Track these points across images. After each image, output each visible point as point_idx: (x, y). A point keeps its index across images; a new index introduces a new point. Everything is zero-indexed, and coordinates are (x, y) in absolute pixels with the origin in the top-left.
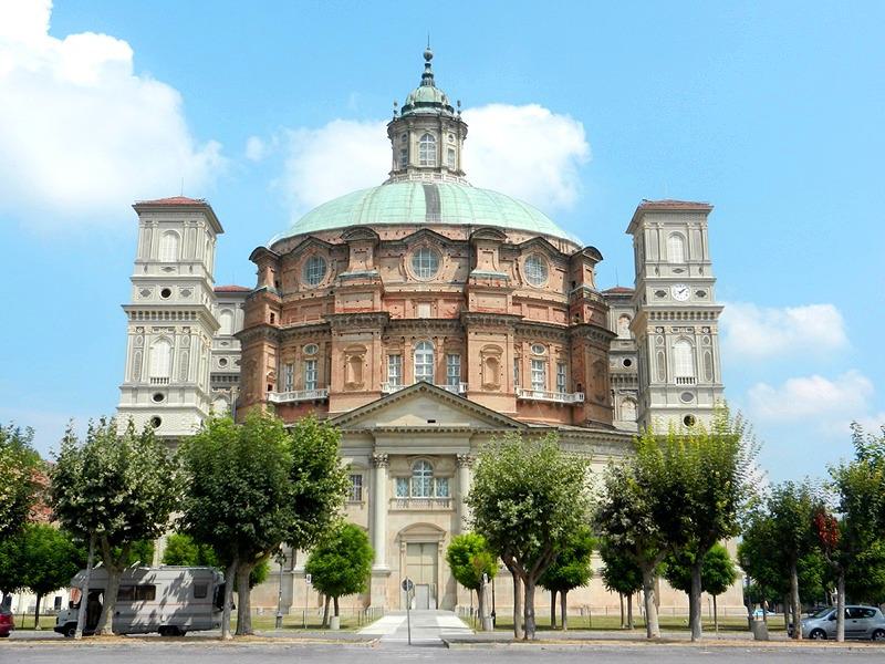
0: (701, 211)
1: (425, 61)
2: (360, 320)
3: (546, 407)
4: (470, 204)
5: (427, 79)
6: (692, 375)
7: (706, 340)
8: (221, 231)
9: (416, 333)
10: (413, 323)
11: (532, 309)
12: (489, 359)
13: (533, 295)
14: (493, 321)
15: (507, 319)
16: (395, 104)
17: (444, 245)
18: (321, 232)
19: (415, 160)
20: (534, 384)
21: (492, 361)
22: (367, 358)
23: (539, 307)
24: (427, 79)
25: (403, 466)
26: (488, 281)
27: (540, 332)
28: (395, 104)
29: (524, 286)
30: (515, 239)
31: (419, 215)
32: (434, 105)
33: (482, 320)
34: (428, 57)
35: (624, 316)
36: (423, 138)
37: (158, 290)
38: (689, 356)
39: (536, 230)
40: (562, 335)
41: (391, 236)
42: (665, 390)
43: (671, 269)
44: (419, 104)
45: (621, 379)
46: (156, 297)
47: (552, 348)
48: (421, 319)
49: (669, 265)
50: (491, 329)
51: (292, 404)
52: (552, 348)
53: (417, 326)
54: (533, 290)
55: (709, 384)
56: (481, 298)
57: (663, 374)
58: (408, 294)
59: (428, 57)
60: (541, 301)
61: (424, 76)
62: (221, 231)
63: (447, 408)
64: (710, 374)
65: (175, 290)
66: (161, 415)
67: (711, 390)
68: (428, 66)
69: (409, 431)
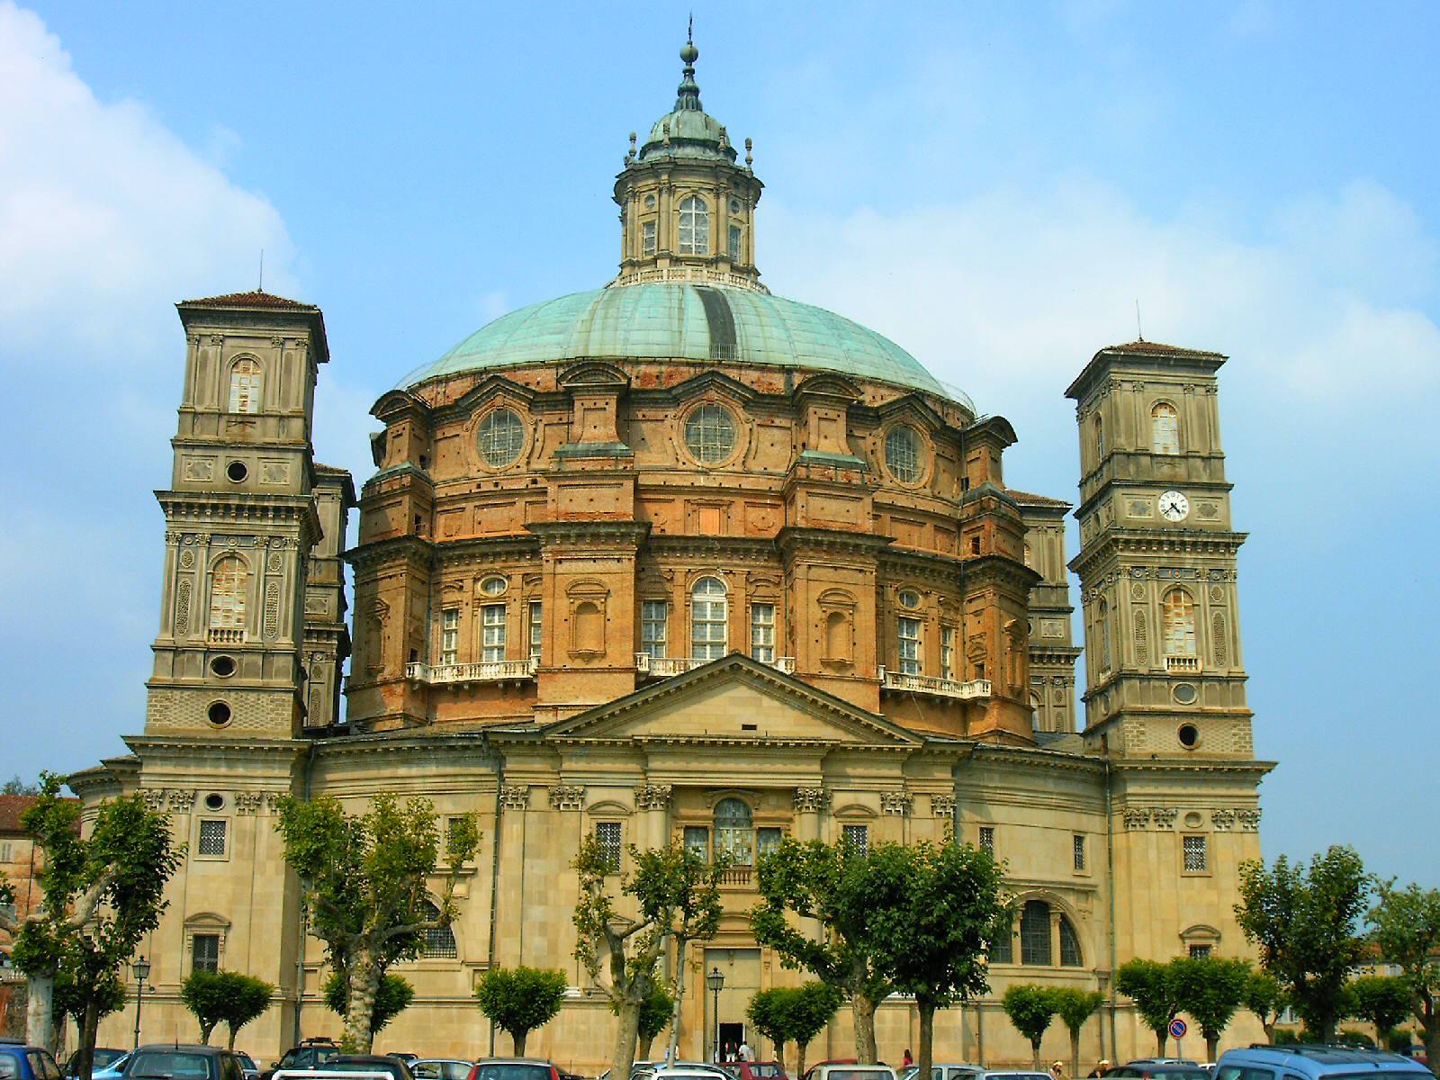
0: (1210, 363)
1: (683, 65)
3: (919, 707)
4: (787, 330)
5: (689, 96)
9: (696, 562)
10: (690, 544)
13: (902, 501)
16: (633, 139)
18: (515, 368)
24: (689, 96)
25: (700, 812)
26: (831, 472)
27: (914, 568)
28: (633, 139)
30: (870, 398)
31: (697, 341)
32: (704, 144)
34: (690, 57)
36: (686, 203)
40: (949, 574)
44: (679, 142)
48: (706, 538)
51: (458, 687)
52: (933, 599)
53: (697, 549)
58: (679, 490)
60: (914, 511)
63: (776, 703)
66: (230, 700)
68: (689, 73)
69: (714, 743)
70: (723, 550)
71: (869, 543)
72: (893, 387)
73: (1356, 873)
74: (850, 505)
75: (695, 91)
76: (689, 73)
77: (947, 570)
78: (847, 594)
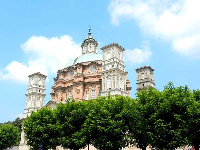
1: (89, 31)
2: (57, 89)
6: (110, 88)
8: (153, 70)
9: (69, 89)
12: (77, 92)
14: (77, 84)
15: (80, 82)
17: (74, 69)
20: (93, 96)
21: (78, 93)
22: (58, 96)
29: (90, 74)
33: (75, 84)
34: (90, 30)
35: (143, 73)
36: (85, 47)
37: (38, 90)
38: (110, 83)
39: (91, 60)
41: (66, 70)
42: (104, 93)
43: (107, 62)
45: (144, 89)
46: (30, 92)
47: (97, 87)
49: (107, 61)
50: (78, 86)
52: (97, 87)
54: (93, 74)
55: (114, 89)
56: (76, 79)
57: (104, 89)
59: (90, 30)
62: (153, 70)
65: (32, 90)
67: (114, 90)
68: (90, 31)
70: (71, 87)
74: (80, 78)
76: (90, 31)
78: (79, 89)
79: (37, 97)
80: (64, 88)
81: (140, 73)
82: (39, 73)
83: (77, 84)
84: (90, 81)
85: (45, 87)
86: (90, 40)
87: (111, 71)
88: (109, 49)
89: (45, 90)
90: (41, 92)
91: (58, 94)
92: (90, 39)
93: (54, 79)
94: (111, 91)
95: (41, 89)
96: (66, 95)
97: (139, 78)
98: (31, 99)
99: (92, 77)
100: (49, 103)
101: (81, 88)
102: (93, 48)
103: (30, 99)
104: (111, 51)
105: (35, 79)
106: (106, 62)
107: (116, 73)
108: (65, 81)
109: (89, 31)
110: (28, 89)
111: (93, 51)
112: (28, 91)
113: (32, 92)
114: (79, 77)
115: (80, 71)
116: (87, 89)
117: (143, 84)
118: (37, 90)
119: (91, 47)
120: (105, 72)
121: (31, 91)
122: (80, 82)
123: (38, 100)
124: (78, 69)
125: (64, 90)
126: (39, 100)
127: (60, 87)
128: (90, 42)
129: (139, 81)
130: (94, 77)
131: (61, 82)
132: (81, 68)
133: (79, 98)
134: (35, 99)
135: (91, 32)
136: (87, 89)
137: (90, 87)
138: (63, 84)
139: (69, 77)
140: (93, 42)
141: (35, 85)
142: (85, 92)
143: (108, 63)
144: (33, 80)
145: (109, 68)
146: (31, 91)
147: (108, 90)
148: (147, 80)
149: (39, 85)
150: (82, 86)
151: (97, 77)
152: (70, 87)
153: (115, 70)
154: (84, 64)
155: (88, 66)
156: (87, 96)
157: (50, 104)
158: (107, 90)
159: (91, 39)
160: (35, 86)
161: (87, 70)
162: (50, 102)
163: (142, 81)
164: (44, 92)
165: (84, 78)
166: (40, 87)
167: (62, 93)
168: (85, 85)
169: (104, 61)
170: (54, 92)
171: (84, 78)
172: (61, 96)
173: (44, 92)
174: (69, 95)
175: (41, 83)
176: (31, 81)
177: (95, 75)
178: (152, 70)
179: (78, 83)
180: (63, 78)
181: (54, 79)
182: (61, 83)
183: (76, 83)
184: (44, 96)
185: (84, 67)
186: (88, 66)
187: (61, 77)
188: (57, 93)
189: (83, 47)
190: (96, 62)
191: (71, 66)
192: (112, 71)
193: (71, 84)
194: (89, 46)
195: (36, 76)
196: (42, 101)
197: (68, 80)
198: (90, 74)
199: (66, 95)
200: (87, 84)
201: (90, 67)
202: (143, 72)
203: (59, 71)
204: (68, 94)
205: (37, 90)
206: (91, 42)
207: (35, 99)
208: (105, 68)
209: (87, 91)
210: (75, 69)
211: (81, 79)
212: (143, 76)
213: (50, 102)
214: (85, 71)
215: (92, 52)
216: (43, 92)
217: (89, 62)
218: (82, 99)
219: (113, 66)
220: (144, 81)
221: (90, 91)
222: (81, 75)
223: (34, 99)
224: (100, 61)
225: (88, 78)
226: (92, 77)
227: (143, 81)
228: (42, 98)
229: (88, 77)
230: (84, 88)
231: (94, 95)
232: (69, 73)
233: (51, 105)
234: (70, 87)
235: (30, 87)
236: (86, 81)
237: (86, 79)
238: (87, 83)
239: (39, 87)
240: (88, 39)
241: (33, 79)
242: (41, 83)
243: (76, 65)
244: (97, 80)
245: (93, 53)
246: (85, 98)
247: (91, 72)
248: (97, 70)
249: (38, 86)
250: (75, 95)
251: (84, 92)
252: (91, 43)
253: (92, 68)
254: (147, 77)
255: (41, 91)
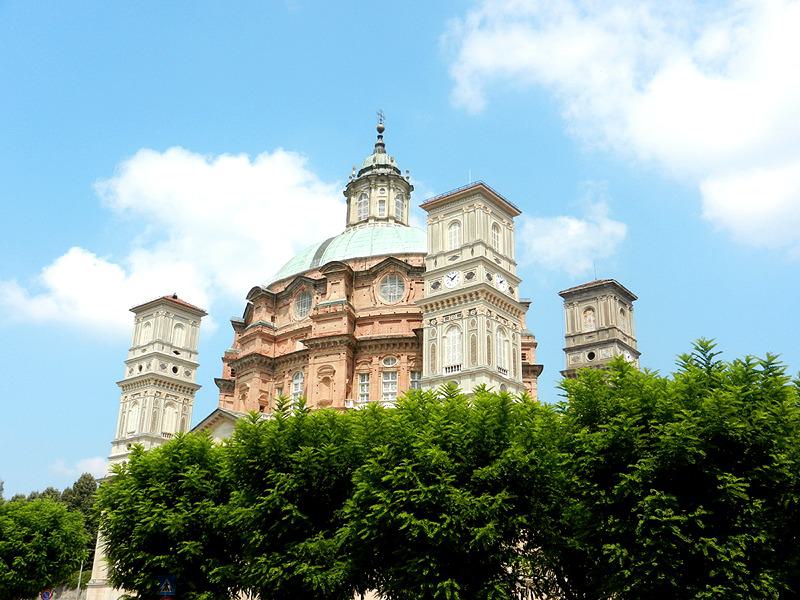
7: (473, 323)
8: (633, 298)
11: (385, 325)
13: (386, 312)
15: (336, 340)
19: (352, 221)
20: (387, 394)
21: (326, 380)
22: (248, 394)
23: (394, 321)
29: (379, 305)
33: (317, 345)
34: (381, 130)
35: (589, 309)
36: (360, 199)
37: (170, 366)
40: (412, 344)
42: (431, 382)
43: (447, 258)
46: (136, 373)
47: (404, 358)
49: (445, 255)
50: (327, 352)
52: (404, 358)
54: (387, 307)
55: (473, 369)
56: (323, 325)
57: (433, 366)
59: (381, 130)
60: (396, 315)
61: (377, 145)
62: (633, 298)
64: (474, 359)
65: (144, 365)
67: (472, 375)
68: (380, 137)
70: (299, 358)
71: (340, 339)
72: (380, 257)
73: (430, 491)
74: (336, 323)
75: (383, 145)
76: (380, 137)
77: (410, 342)
79: (164, 393)
80: (271, 359)
81: (578, 309)
82: (175, 297)
83: (323, 343)
84: (375, 335)
85: (197, 354)
86: (382, 170)
87: (461, 294)
88: (454, 207)
89: (195, 366)
90: (180, 375)
91: (248, 385)
92: (379, 166)
93: (236, 325)
94: (459, 377)
95: (182, 362)
96: (281, 389)
97: (573, 328)
98: (140, 401)
99: (383, 319)
100: (211, 419)
101: (338, 363)
102: (393, 203)
103: (136, 403)
104: (466, 215)
105: (156, 323)
106: (444, 262)
107: (481, 307)
108: (276, 334)
109: (379, 137)
110: (130, 362)
111: (390, 213)
112: (128, 369)
113: (144, 372)
114: (335, 316)
115: (336, 292)
116: (365, 367)
117: (590, 350)
118: (163, 367)
119: (382, 198)
120: (438, 300)
121: (141, 368)
122: (336, 340)
123: (166, 405)
124: (329, 285)
125: (271, 367)
126: (170, 404)
127: (255, 354)
128: (383, 178)
129: (576, 338)
130: (396, 318)
131: (262, 335)
132: (342, 283)
133: (330, 403)
134: (157, 402)
135: (384, 141)
136: (363, 368)
137: (375, 359)
138: (270, 343)
139: (294, 316)
140: (392, 178)
141: (156, 345)
142: (357, 380)
143: (452, 263)
144: (148, 324)
145: (453, 283)
146: (141, 368)
147: (448, 374)
148: (606, 337)
149: (171, 346)
150: (344, 356)
151: (404, 320)
152: (295, 359)
153: (477, 294)
154: (357, 268)
155: (372, 274)
156: (362, 396)
157: (214, 422)
158: (445, 374)
159: (385, 166)
160: (156, 348)
161: (365, 290)
162: (216, 415)
163: (584, 341)
164: (193, 372)
165: (355, 322)
166: (176, 353)
167: (265, 382)
168: (356, 349)
169: (436, 257)
170: (233, 374)
171: (355, 322)
172: (261, 391)
173: (193, 372)
174: (293, 389)
175: (180, 337)
176: (144, 331)
177: (399, 311)
178: (626, 297)
179: (329, 343)
180: (268, 319)
181: (236, 325)
182: (259, 340)
183: (319, 342)
184: (191, 389)
185: (353, 276)
186: (372, 274)
187: (262, 316)
188: (246, 378)
189: (354, 200)
190: (403, 259)
191: (304, 273)
192: (465, 297)
193: (299, 346)
194: (376, 194)
195: (162, 311)
196: (185, 409)
197: (289, 330)
198: (379, 305)
199: (281, 389)
200: (365, 347)
201: (377, 280)
202: (592, 304)
203: (255, 293)
204: (286, 385)
205: (163, 367)
206: (382, 178)
207: (157, 402)
208: (438, 284)
209: (363, 375)
210: (320, 285)
211: (341, 327)
212: (592, 318)
213: (216, 415)
214: (357, 293)
215: (387, 219)
216: (188, 374)
217: (373, 258)
218: (342, 405)
219: (470, 276)
220: (596, 339)
221: (375, 375)
222: (339, 309)
223: (150, 400)
224: (418, 255)
225: (368, 321)
226: (383, 319)
227: (590, 341)
228: (182, 397)
229: (370, 318)
230: (352, 364)
231: (390, 389)
232: (293, 303)
233: (217, 427)
234: (295, 359)
235: (139, 354)
236: (362, 333)
237: (360, 325)
238: (365, 344)
239: (174, 355)
240: (371, 168)
241: (152, 321)
242: (180, 337)
243: (321, 269)
244: (403, 329)
245: (391, 221)
246: (355, 403)
247: (380, 298)
248: (407, 291)
249: (168, 351)
250: (316, 389)
251: (350, 377)
252: (386, 183)
253: (385, 281)
254: (607, 323)
255: (181, 369)
